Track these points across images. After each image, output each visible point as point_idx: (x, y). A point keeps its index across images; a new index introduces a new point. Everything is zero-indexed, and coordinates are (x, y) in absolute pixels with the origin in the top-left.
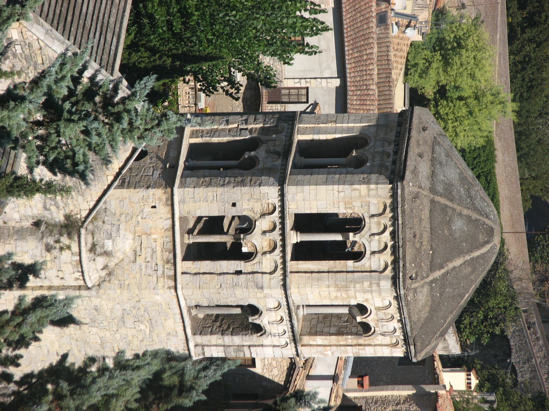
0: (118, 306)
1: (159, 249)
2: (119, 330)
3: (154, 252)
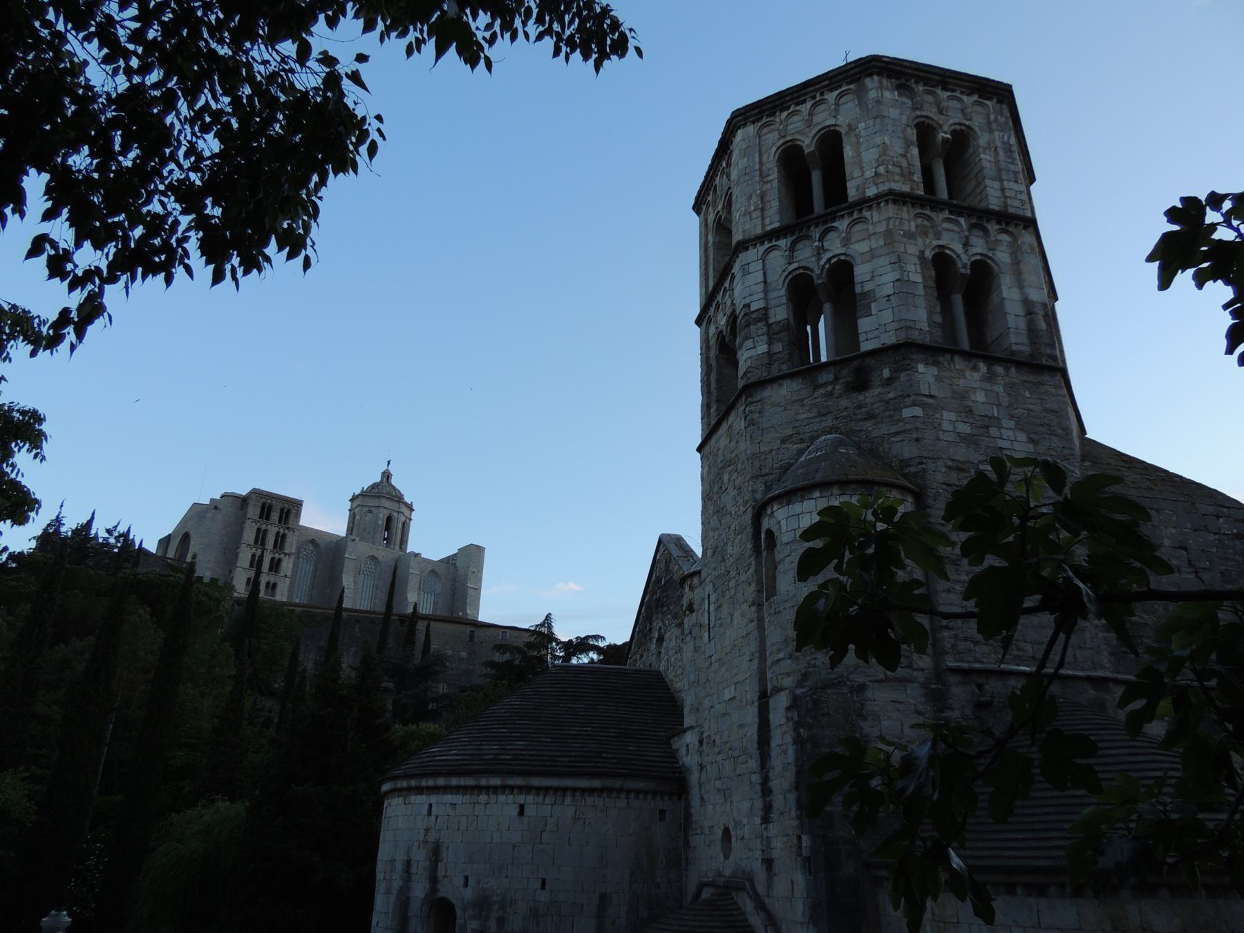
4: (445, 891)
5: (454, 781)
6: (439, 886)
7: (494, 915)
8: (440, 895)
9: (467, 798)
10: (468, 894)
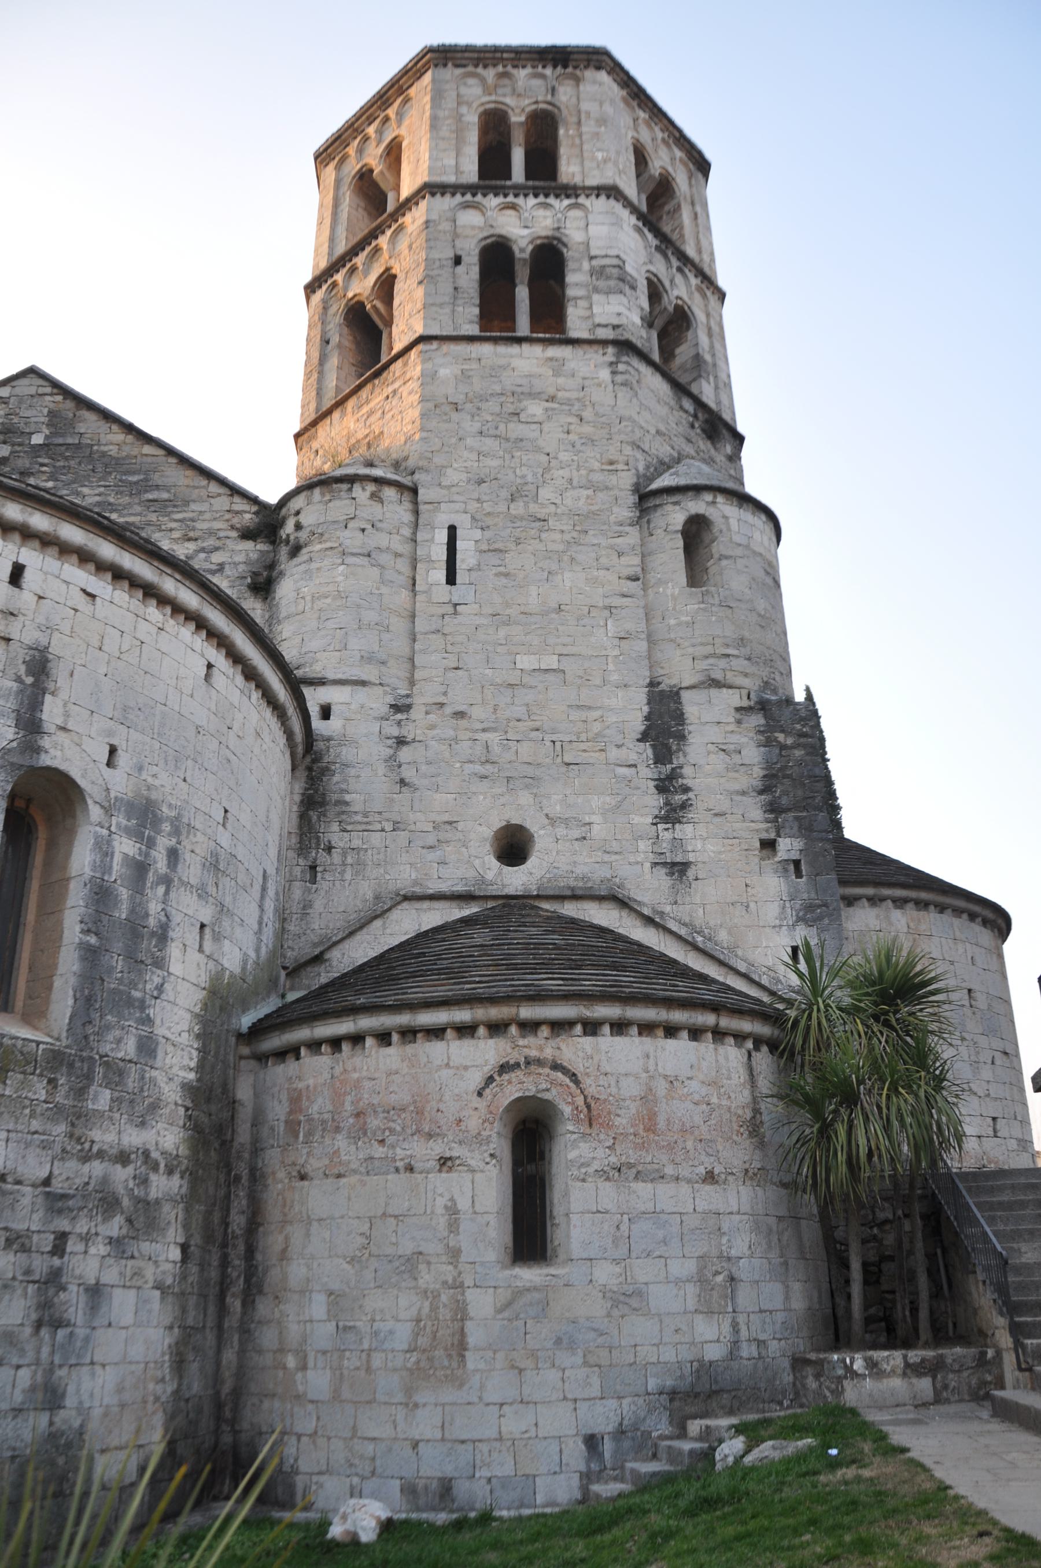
0: (469, 441)
1: (365, 409)
2: (547, 450)
3: (371, 413)
4: (57, 753)
5: (107, 550)
6: (46, 742)
7: (163, 843)
8: (45, 760)
9: (121, 595)
10: (120, 782)
